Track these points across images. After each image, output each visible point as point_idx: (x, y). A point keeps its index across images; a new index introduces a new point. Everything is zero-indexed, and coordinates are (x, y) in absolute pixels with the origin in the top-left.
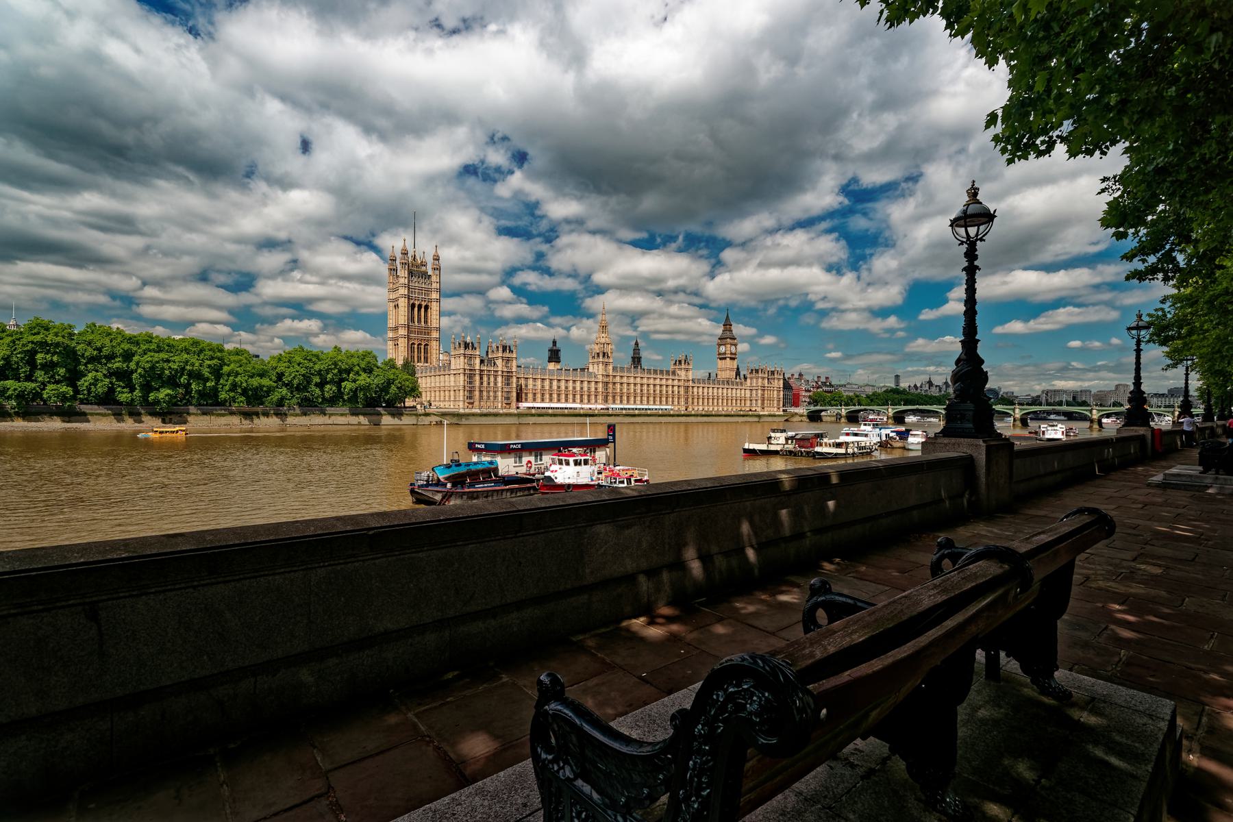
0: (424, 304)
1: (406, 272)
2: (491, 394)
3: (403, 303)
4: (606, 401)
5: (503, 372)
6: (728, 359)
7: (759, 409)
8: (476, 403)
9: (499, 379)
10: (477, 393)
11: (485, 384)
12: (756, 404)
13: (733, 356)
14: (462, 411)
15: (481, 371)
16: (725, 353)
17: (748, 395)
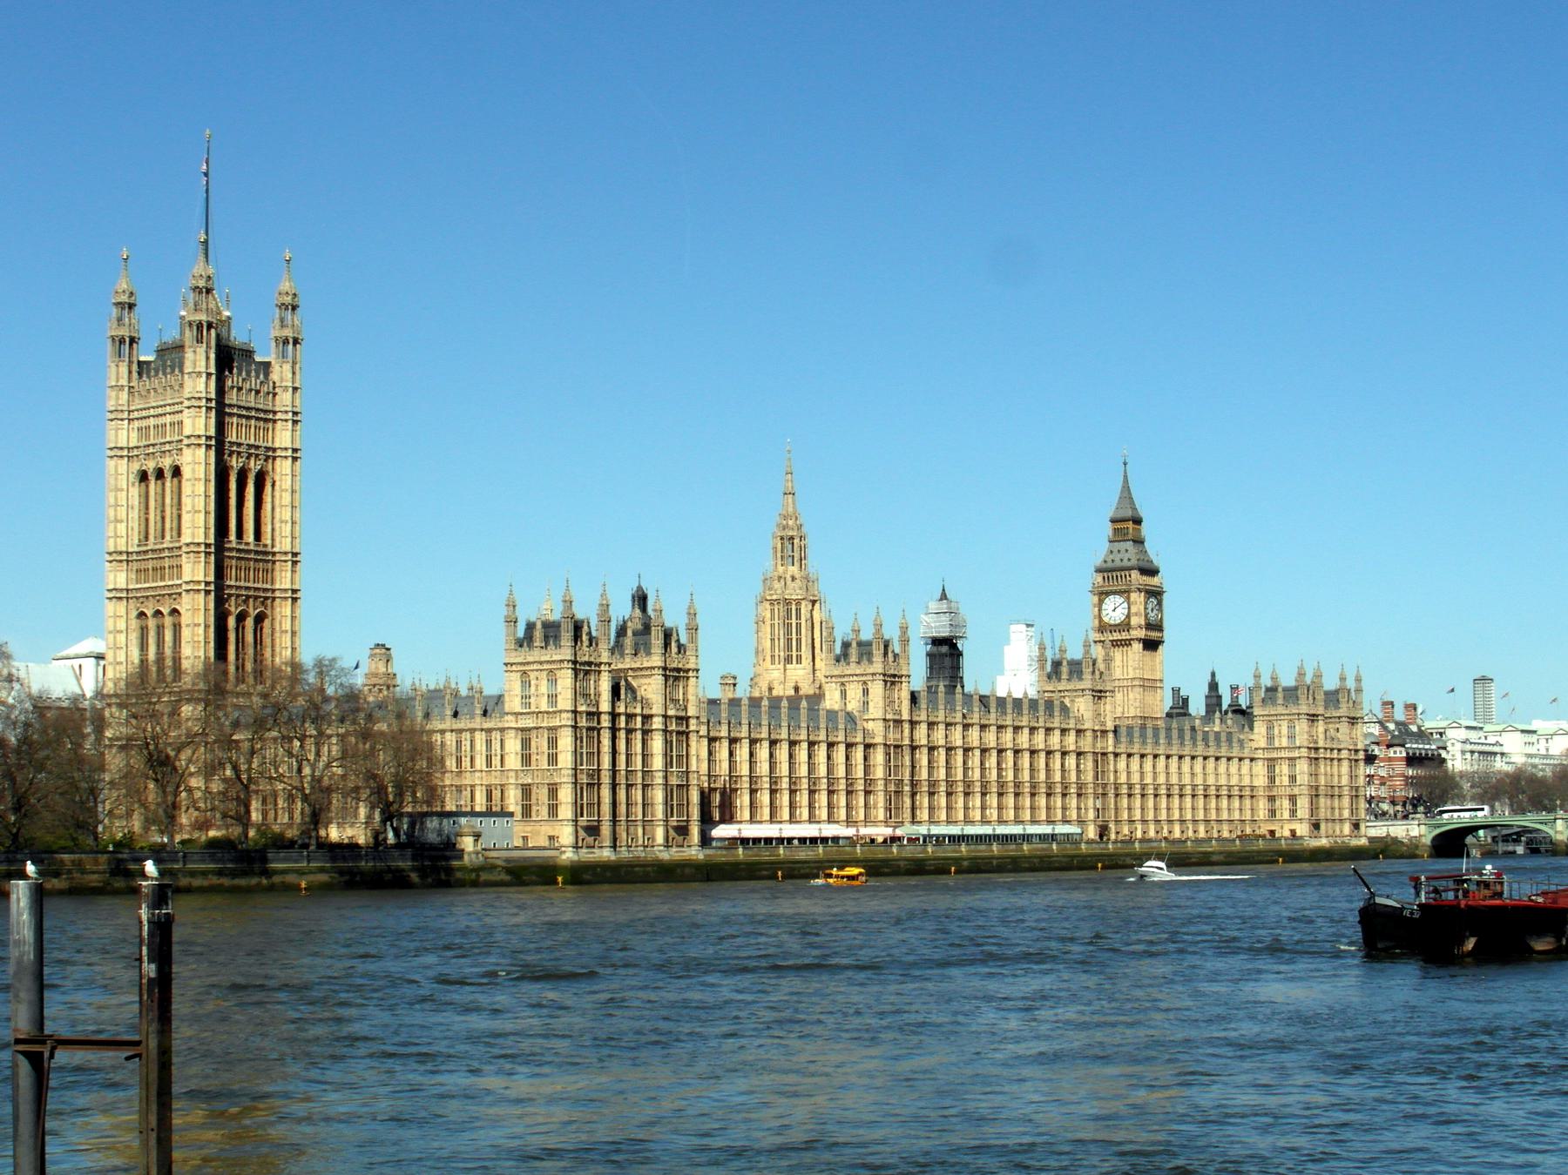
0: (254, 466)
1: (213, 356)
2: (638, 795)
3: (197, 465)
4: (892, 810)
5: (665, 717)
6: (1138, 647)
7: (1302, 829)
8: (606, 830)
9: (657, 744)
10: (606, 793)
11: (622, 759)
12: (1293, 812)
13: (1154, 635)
14: (568, 855)
15: (614, 716)
16: (1125, 625)
17: (1261, 781)
